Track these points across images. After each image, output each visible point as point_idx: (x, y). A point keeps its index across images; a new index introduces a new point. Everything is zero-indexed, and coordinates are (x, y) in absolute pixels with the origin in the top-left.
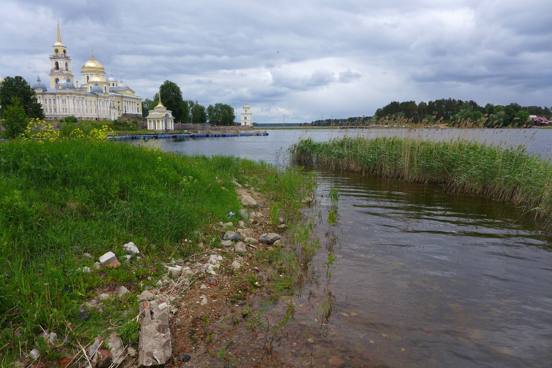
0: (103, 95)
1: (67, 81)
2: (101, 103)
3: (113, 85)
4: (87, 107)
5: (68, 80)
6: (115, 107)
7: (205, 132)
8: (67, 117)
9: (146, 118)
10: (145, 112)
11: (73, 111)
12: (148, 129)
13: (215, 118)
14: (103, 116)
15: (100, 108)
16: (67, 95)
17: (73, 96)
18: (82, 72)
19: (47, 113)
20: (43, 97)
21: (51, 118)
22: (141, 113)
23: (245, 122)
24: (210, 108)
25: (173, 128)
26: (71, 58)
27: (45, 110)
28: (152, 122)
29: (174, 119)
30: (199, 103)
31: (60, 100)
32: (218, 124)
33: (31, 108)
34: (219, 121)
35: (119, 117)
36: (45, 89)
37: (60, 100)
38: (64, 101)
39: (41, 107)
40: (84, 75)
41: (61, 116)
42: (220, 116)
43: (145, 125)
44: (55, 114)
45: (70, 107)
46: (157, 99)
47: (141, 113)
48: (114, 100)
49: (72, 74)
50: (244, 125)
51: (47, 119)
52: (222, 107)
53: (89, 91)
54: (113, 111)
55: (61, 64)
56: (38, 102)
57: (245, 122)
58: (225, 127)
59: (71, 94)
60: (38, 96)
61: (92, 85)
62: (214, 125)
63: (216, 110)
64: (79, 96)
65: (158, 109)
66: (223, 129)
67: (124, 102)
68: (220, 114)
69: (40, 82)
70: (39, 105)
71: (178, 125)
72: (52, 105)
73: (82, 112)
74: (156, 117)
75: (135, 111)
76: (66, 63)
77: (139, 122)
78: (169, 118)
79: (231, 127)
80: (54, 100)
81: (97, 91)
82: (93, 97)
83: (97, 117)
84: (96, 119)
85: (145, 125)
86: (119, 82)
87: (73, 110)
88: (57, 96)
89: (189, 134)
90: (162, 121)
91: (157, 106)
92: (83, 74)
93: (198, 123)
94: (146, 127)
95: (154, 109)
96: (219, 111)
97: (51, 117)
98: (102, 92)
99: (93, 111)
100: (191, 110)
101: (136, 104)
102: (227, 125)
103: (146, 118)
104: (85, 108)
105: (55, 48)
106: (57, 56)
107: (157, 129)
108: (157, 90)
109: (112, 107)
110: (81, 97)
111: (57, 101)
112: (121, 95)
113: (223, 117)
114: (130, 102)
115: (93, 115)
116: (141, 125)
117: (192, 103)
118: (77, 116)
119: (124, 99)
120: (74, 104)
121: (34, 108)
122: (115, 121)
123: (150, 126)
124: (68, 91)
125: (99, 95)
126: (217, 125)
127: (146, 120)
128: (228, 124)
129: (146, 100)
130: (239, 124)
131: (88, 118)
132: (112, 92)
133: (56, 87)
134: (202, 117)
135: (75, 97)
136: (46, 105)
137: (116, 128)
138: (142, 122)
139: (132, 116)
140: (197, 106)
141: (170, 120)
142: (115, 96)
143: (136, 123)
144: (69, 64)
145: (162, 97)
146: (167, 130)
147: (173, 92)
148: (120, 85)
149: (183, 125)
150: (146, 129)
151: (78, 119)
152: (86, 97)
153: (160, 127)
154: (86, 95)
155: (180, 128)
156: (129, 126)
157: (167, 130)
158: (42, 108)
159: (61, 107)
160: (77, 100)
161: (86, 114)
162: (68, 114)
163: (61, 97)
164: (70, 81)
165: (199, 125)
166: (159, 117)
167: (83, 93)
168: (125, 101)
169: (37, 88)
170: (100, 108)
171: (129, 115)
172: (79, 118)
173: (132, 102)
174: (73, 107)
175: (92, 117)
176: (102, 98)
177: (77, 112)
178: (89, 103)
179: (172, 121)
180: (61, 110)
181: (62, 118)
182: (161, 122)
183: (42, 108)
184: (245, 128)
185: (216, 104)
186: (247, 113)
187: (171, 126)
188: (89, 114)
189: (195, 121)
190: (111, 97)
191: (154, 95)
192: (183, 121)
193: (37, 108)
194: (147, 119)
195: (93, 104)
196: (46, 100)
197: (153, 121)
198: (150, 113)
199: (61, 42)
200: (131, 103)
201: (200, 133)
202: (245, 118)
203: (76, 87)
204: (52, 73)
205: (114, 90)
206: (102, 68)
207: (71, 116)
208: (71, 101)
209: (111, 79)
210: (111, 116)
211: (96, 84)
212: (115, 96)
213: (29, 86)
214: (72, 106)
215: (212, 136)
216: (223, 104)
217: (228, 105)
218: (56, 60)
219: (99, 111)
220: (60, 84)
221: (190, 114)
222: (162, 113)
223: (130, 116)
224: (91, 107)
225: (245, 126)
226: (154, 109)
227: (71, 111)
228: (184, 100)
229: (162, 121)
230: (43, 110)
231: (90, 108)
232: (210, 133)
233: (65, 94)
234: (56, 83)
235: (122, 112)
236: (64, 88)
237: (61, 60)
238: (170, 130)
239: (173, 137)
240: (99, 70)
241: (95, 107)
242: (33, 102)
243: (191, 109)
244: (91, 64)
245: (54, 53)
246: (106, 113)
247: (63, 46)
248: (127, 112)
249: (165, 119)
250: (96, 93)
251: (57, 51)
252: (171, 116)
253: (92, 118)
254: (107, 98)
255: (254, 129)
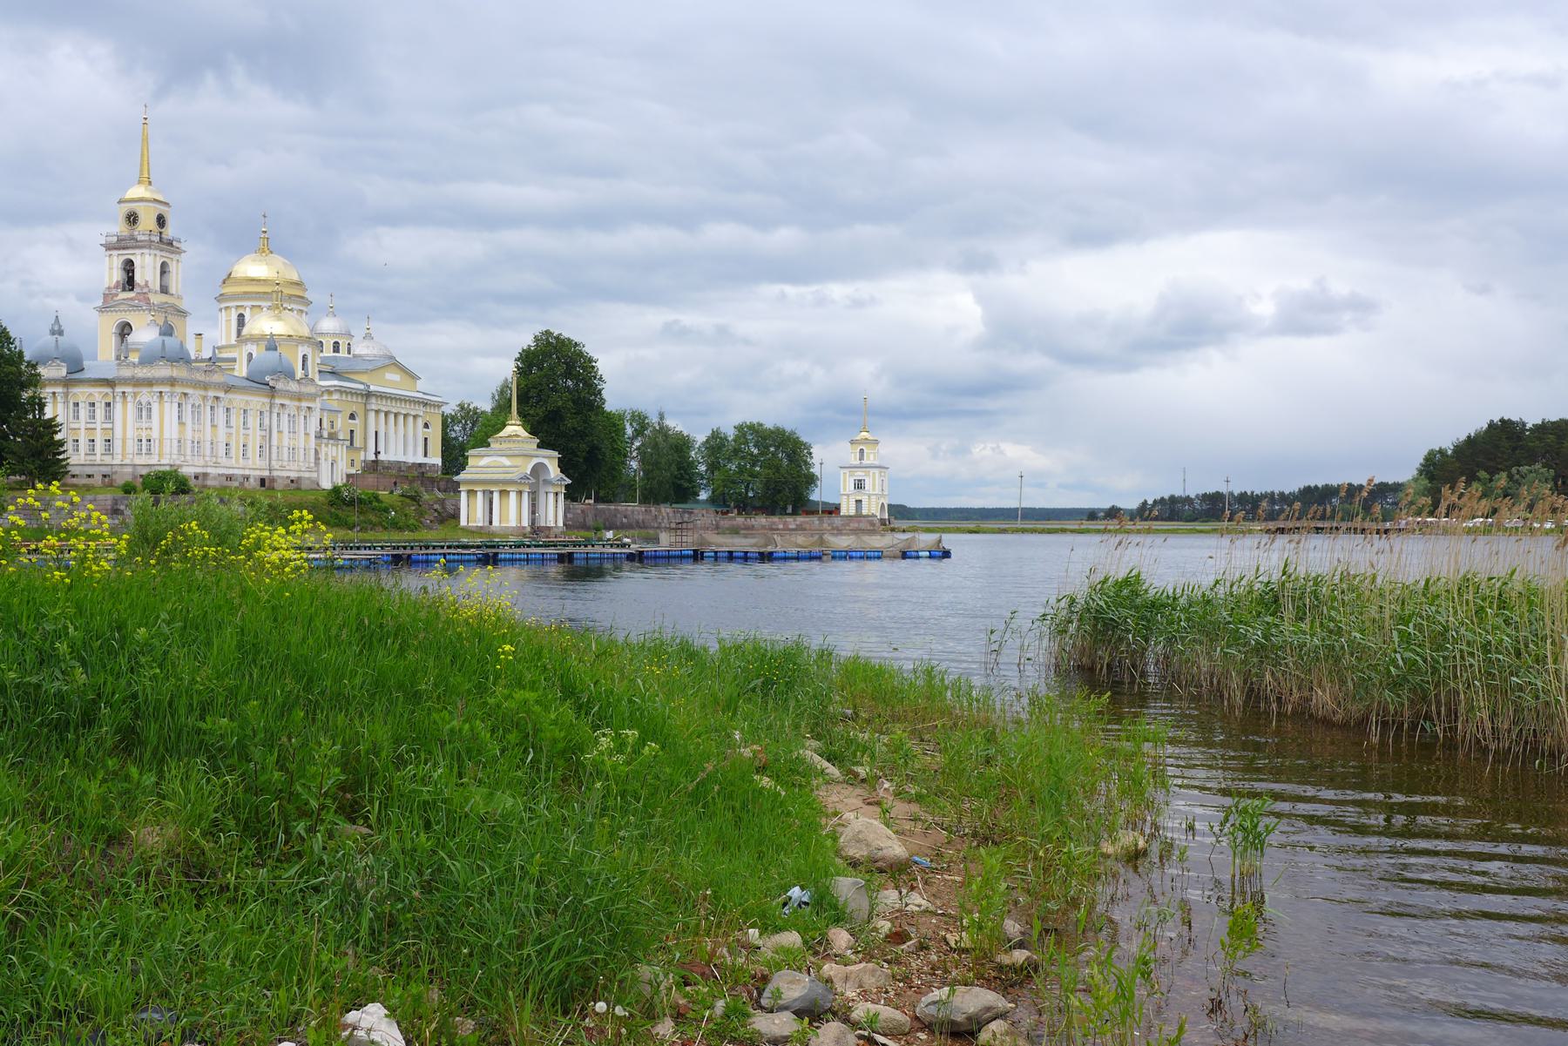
0: (293, 387)
1: (160, 334)
2: (285, 418)
3: (336, 347)
5: (167, 331)
6: (336, 433)
7: (689, 542)
8: (149, 475)
9: (456, 478)
10: (454, 457)
11: (176, 452)
12: (463, 522)
13: (733, 482)
14: (288, 468)
15: (280, 440)
16: (157, 389)
17: (179, 390)
18: (221, 298)
19: (76, 458)
20: (66, 395)
21: (89, 476)
22: (438, 461)
23: (859, 502)
24: (716, 443)
25: (560, 524)
26: (183, 246)
27: (69, 446)
28: (480, 495)
29: (567, 487)
30: (670, 422)
31: (131, 408)
32: (744, 507)
33: (21, 436)
34: (751, 494)
35: (349, 476)
36: (76, 366)
37: (130, 406)
38: (144, 411)
39: (56, 433)
40: (227, 308)
41: (130, 470)
42: (752, 475)
43: (450, 508)
44: (108, 460)
45: (167, 435)
46: (502, 407)
47: (436, 460)
48: (335, 406)
49: (183, 305)
50: (852, 512)
51: (75, 481)
52: (765, 439)
53: (242, 370)
54: (329, 451)
55: (142, 267)
56: (49, 413)
57: (859, 502)
58: (775, 519)
59: (172, 382)
60: (49, 390)
61: (251, 348)
62: (728, 512)
63: (736, 451)
64: (203, 393)
65: (504, 446)
66: (763, 527)
67: (372, 415)
68: (754, 465)
69: (60, 338)
70: (51, 426)
71: (583, 511)
72: (98, 426)
73: (208, 452)
74: (496, 477)
75: (415, 453)
76: (164, 265)
77: (426, 497)
78: (547, 482)
79: (800, 519)
80: (108, 405)
81: (273, 372)
82: (252, 394)
83: (266, 473)
84: (263, 482)
85: (450, 508)
86: (358, 333)
87: (175, 444)
88: (119, 389)
89: (624, 546)
90: (520, 493)
91: (501, 434)
92: (223, 305)
93: (663, 503)
94: (455, 516)
95: (489, 445)
96: (752, 454)
97: (89, 471)
98: (290, 375)
99: (253, 450)
100: (638, 449)
101: (420, 423)
102: (784, 512)
103: (456, 478)
105: (126, 208)
106: (133, 238)
107: (496, 523)
108: (505, 369)
109: (325, 435)
110: (211, 393)
111: (118, 408)
112: (362, 387)
113: (767, 485)
114: (396, 415)
115: (252, 466)
116: (436, 506)
117: (640, 421)
118: (188, 471)
119: (374, 404)
120: (181, 424)
121: (31, 437)
122: (336, 490)
123: (472, 513)
124: (163, 371)
125: (280, 386)
126: (739, 514)
127: (455, 488)
128: (785, 509)
129: (462, 406)
130: (833, 510)
131: (230, 478)
132: (329, 376)
133: (118, 358)
134: (682, 478)
135: (185, 394)
136: (76, 426)
137: (337, 517)
138: (440, 495)
139: (400, 470)
140: (663, 431)
141: (553, 490)
142: (341, 391)
143: (415, 499)
144: (172, 267)
145: (523, 398)
146: (536, 529)
147: (568, 374)
148: (360, 349)
149: (603, 511)
150: (452, 522)
151: (192, 482)
152: (230, 396)
153: (511, 515)
154: (229, 389)
155: (590, 521)
156: (386, 510)
157: (536, 529)
158: (58, 437)
159: (129, 434)
160: (193, 406)
161: (223, 461)
162: (154, 461)
164: (171, 335)
165: (666, 510)
166: (508, 477)
167: (217, 378)
168: (377, 412)
169: (46, 360)
170: (280, 440)
171: (388, 468)
172: (196, 477)
173: (406, 416)
174: (175, 436)
175: (247, 472)
176: (291, 399)
177: (189, 452)
178: (236, 420)
179: (557, 494)
180: (131, 446)
181: (129, 478)
182: (513, 496)
183: (58, 437)
184: (854, 525)
185: (740, 428)
186: (865, 462)
187: (553, 513)
188: (237, 461)
189: (652, 496)
190: (325, 397)
191: (494, 386)
192: (602, 493)
193: (41, 436)
194: (458, 484)
195: (253, 421)
196: (77, 405)
197: (484, 492)
198: (471, 461)
199: (150, 183)
200: (401, 418)
201: (666, 541)
202: (859, 485)
203: (193, 357)
204: (108, 304)
205: (337, 369)
206: (298, 284)
207: (168, 468)
208: (171, 410)
209: (328, 325)
210: (318, 471)
211: (272, 344)
212: (341, 392)
213: (21, 354)
214: (172, 430)
215: (716, 557)
216: (769, 424)
217: (788, 429)
218: (127, 254)
219: (274, 450)
220: (134, 344)
221: (634, 464)
222: (518, 461)
225: (858, 515)
226: (488, 445)
227: (167, 450)
228: (611, 405)
229: (520, 493)
230: (61, 443)
231: (242, 437)
232: (710, 544)
233: (149, 383)
234: (119, 339)
235: (362, 453)
236: (148, 360)
237: (146, 251)
238: (549, 528)
239: (561, 558)
240: (287, 291)
241: (259, 433)
242: (26, 413)
243: (637, 444)
244: (254, 268)
245: (119, 228)
246: (302, 458)
247: (156, 201)
248: (382, 457)
249: (531, 486)
250: (267, 379)
251: (132, 219)
252: (554, 471)
253: (247, 478)
254: (307, 400)
255: (893, 530)
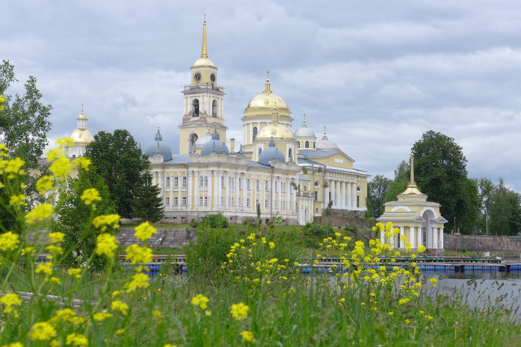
2: (279, 185)
4: (249, 194)
29: (445, 225)
31: (197, 179)
35: (315, 218)
38: (203, 181)
45: (215, 195)
53: (256, 158)
61: (262, 146)
80: (185, 178)
88: (191, 169)
101: (355, 187)
104: (245, 196)
109: (302, 194)
119: (328, 177)
120: (223, 188)
132: (303, 161)
135: (226, 172)
139: (344, 215)
159: (196, 194)
161: (246, 209)
162: (209, 209)
163: (199, 172)
170: (277, 197)
174: (220, 195)
177: (227, 204)
179: (439, 229)
182: (412, 230)
195: (262, 187)
200: (344, 184)
208: (218, 180)
214: (218, 192)
219: (274, 202)
223: (341, 216)
224: (258, 195)
227: (216, 203)
229: (416, 228)
241: (265, 193)
246: (289, 208)
249: (423, 223)
250: (270, 162)
252: (437, 214)
